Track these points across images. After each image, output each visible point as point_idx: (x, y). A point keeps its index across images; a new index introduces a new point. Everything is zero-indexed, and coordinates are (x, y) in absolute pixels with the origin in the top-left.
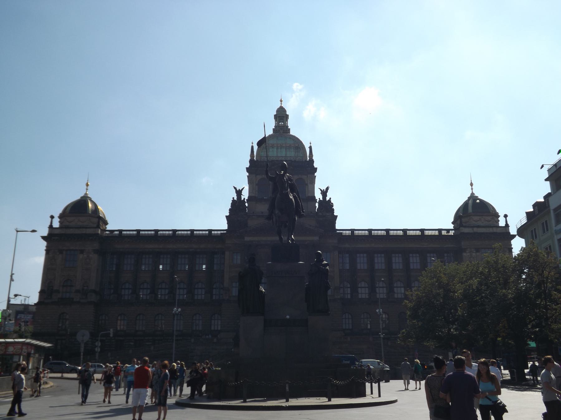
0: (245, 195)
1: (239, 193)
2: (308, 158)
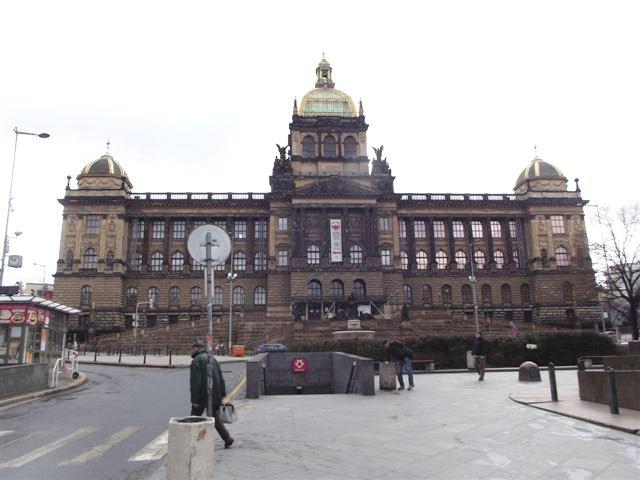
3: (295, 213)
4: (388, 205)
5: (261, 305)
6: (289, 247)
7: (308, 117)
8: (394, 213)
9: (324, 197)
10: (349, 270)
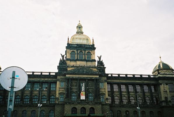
3: (67, 81)
4: (103, 78)
6: (64, 94)
7: (73, 44)
9: (79, 74)
10: (88, 103)
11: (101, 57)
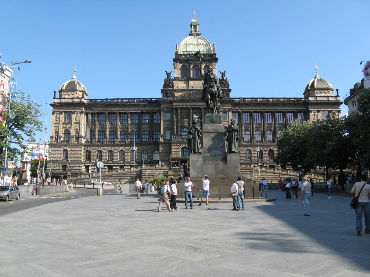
0: (173, 76)
1: (168, 75)
2: (213, 53)
5: (157, 160)
8: (229, 110)
11: (224, 74)
